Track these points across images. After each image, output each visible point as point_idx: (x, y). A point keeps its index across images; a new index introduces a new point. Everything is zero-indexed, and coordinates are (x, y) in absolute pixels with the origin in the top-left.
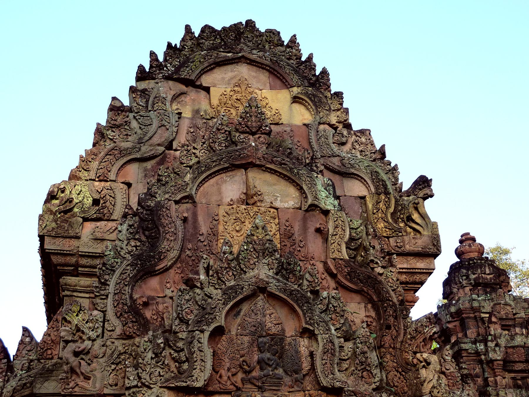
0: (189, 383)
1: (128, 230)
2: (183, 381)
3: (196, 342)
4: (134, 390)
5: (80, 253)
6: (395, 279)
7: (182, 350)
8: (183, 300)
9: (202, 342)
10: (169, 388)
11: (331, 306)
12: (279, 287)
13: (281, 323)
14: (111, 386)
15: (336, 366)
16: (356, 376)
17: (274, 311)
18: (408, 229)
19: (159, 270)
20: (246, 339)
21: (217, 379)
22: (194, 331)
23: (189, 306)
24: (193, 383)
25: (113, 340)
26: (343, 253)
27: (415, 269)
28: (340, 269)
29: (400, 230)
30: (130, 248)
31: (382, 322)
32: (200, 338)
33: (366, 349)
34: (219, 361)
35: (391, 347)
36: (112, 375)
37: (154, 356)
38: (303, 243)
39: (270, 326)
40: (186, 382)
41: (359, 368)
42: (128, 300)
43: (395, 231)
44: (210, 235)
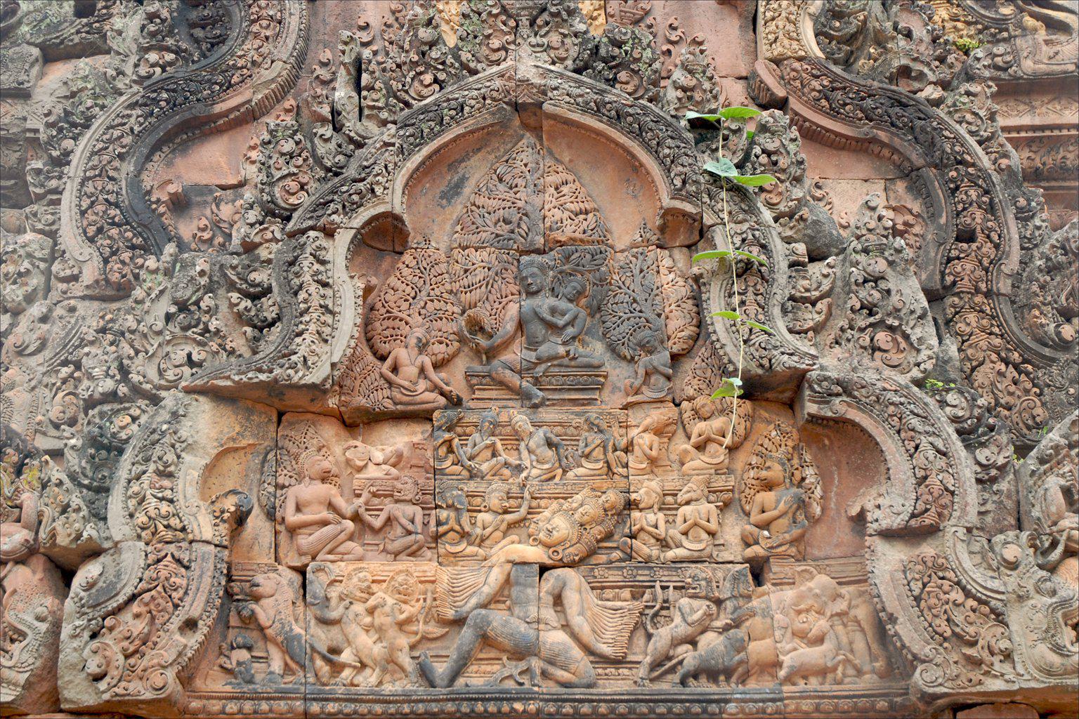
0: (277, 371)
1: (143, 28)
2: (260, 370)
3: (306, 263)
4: (106, 408)
5: (28, 135)
6: (982, 113)
7: (267, 291)
8: (275, 156)
9: (328, 257)
10: (219, 396)
11: (757, 150)
12: (580, 100)
13: (595, 210)
14: (57, 427)
15: (777, 311)
16: (850, 345)
17: (570, 178)
18: (1029, 21)
19: (225, 114)
20: (477, 257)
21: (382, 375)
22: (303, 232)
23: (295, 170)
24: (291, 372)
25: (72, 302)
26: (804, 42)
27: (1060, 127)
28: (798, 84)
29: (1001, 23)
30: (143, 71)
31: (943, 220)
32: (320, 248)
33: (881, 266)
34: (390, 323)
35: (978, 291)
36: (61, 394)
37: (173, 309)
38: (679, 32)
39: (557, 218)
40: (271, 371)
41: (862, 324)
42: (124, 192)
43: (986, 28)
44: (389, 26)
